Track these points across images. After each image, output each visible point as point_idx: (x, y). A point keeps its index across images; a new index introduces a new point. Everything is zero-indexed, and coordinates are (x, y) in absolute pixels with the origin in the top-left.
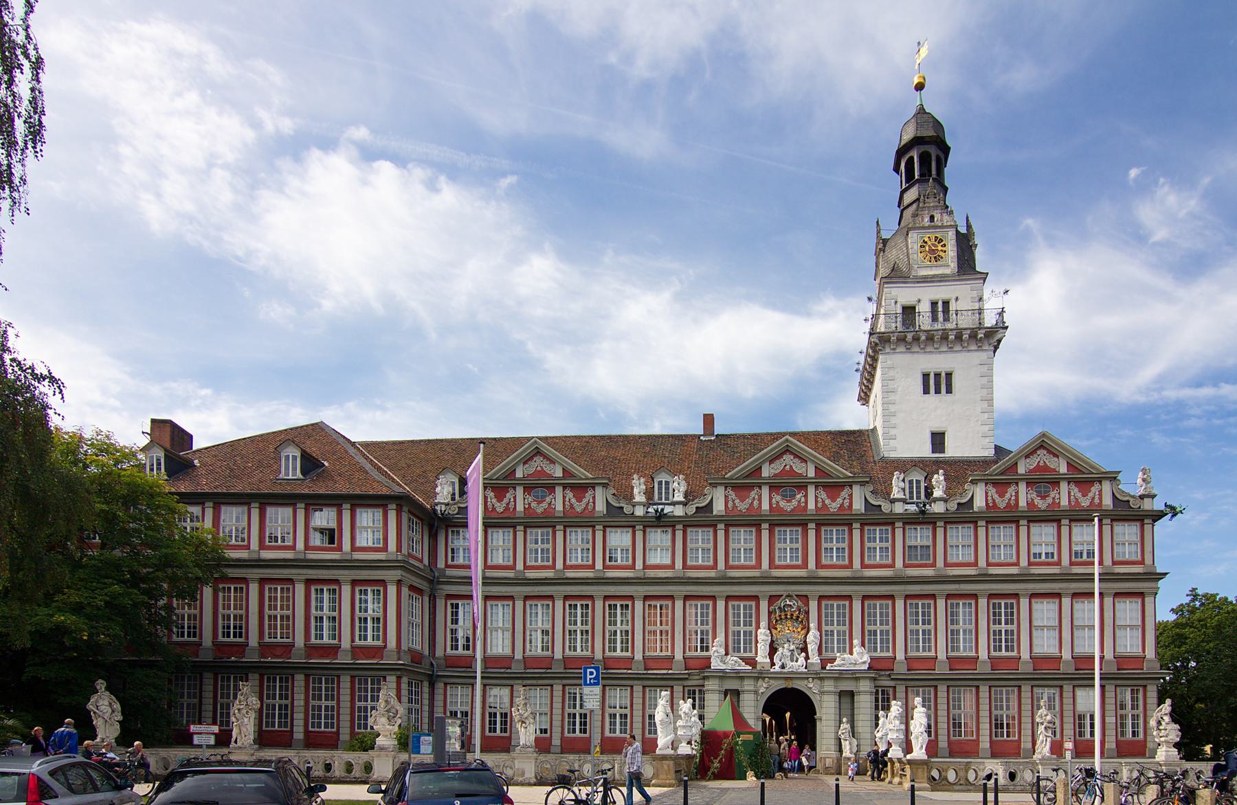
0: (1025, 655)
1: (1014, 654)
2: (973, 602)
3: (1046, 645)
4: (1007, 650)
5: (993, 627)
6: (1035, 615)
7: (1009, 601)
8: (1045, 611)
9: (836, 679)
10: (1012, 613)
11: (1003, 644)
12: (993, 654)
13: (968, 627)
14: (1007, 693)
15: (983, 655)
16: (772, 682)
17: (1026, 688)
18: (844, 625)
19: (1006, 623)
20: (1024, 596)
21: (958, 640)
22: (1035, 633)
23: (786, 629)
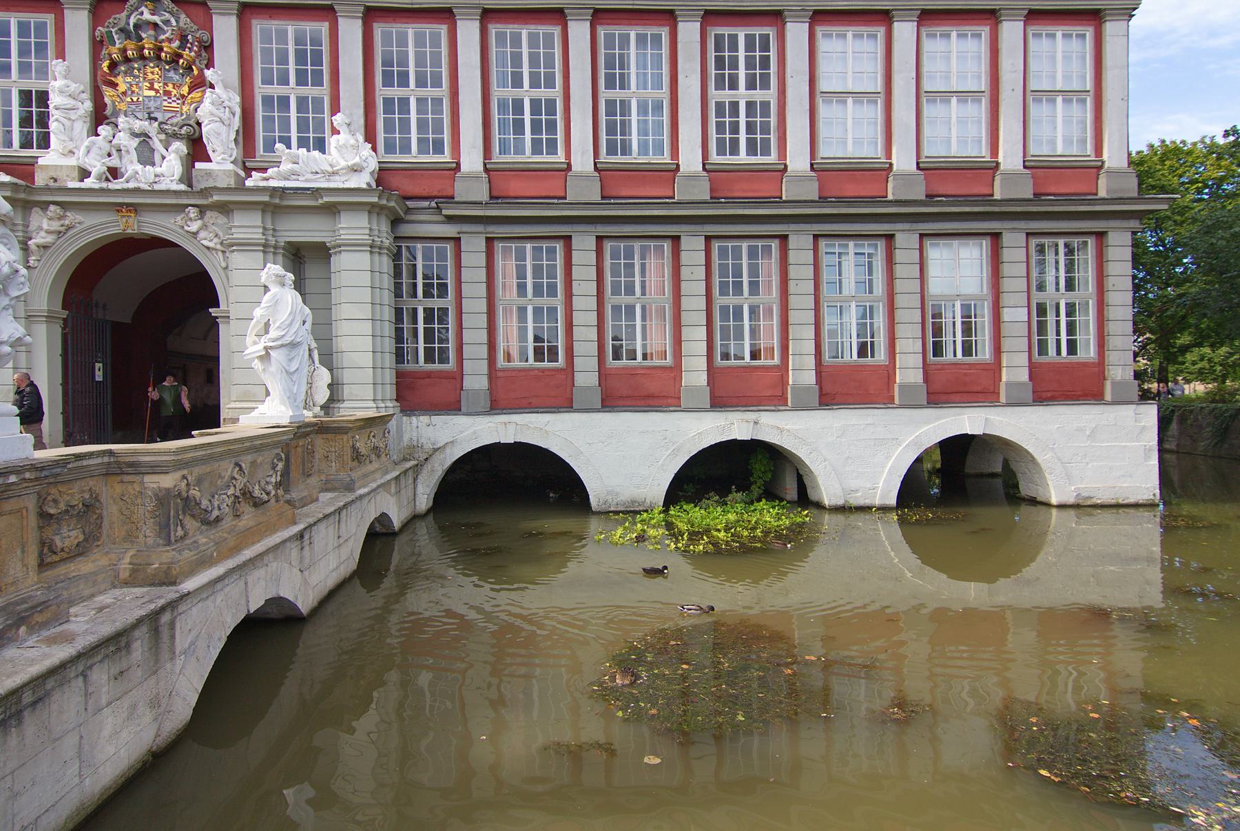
0: (798, 161)
1: (773, 158)
2: (664, 32)
3: (851, 135)
4: (752, 150)
5: (715, 95)
6: (823, 67)
7: (757, 31)
8: (849, 57)
9: (264, 208)
10: (765, 62)
11: (743, 137)
12: (714, 158)
13: (651, 94)
14: (753, 253)
15: (690, 161)
16: (71, 217)
17: (800, 241)
18: (318, 82)
19: (751, 85)
20: (798, 15)
21: (625, 127)
22: (823, 111)
23: (143, 87)
